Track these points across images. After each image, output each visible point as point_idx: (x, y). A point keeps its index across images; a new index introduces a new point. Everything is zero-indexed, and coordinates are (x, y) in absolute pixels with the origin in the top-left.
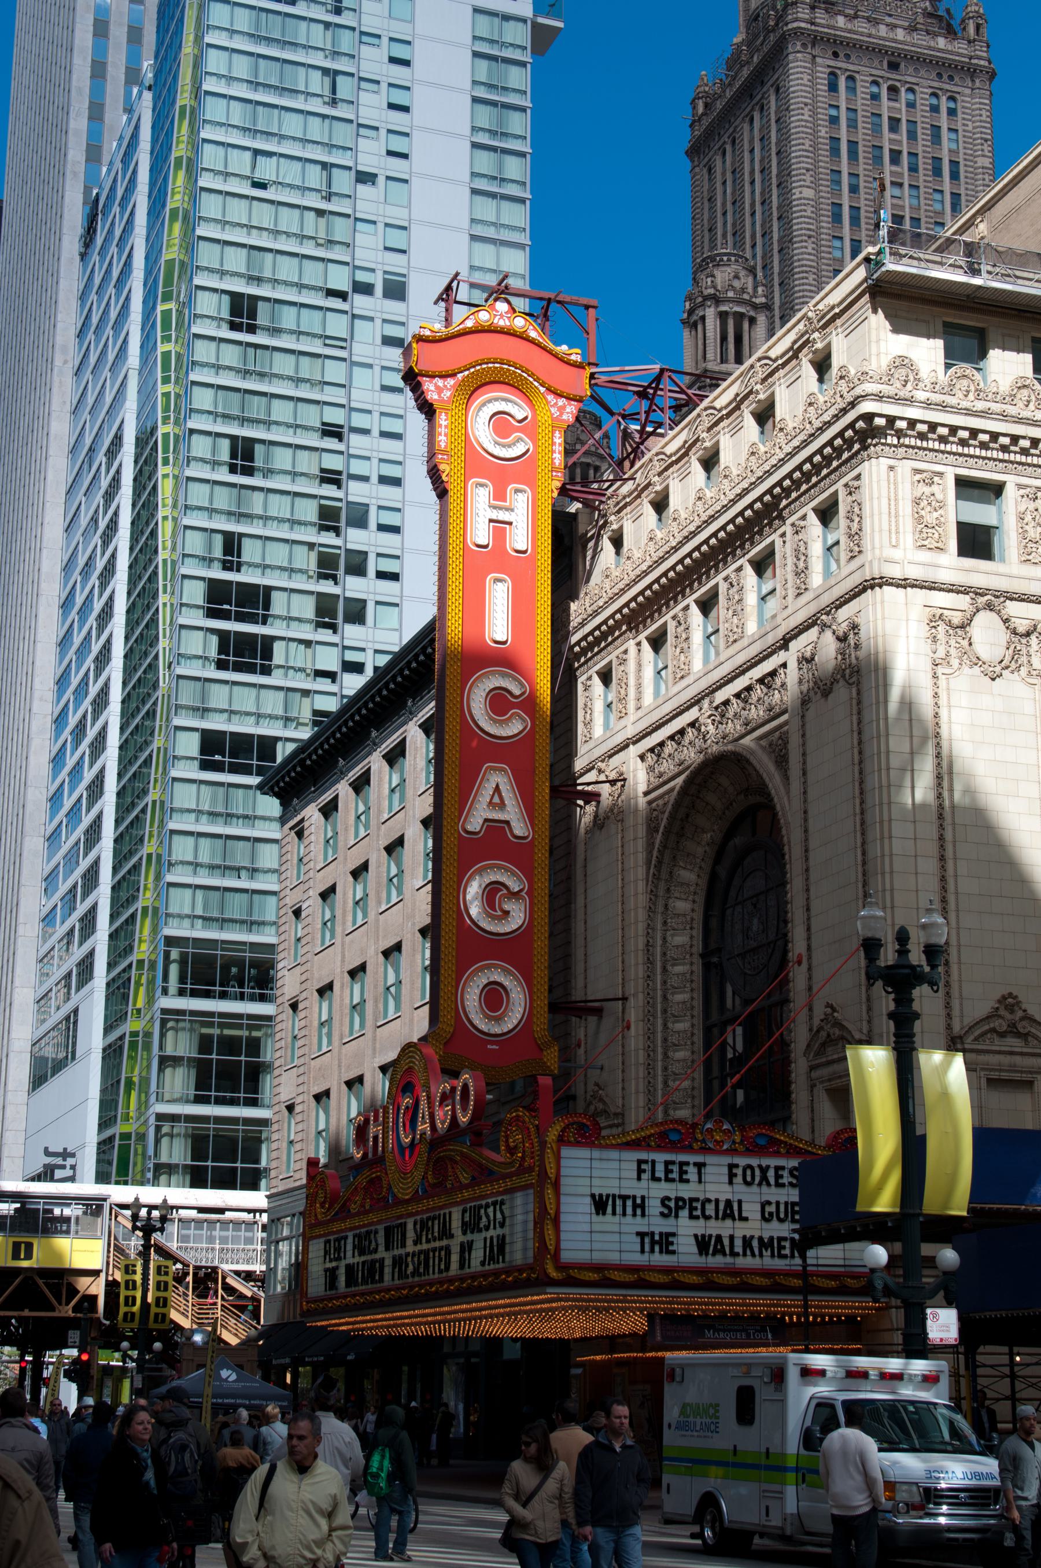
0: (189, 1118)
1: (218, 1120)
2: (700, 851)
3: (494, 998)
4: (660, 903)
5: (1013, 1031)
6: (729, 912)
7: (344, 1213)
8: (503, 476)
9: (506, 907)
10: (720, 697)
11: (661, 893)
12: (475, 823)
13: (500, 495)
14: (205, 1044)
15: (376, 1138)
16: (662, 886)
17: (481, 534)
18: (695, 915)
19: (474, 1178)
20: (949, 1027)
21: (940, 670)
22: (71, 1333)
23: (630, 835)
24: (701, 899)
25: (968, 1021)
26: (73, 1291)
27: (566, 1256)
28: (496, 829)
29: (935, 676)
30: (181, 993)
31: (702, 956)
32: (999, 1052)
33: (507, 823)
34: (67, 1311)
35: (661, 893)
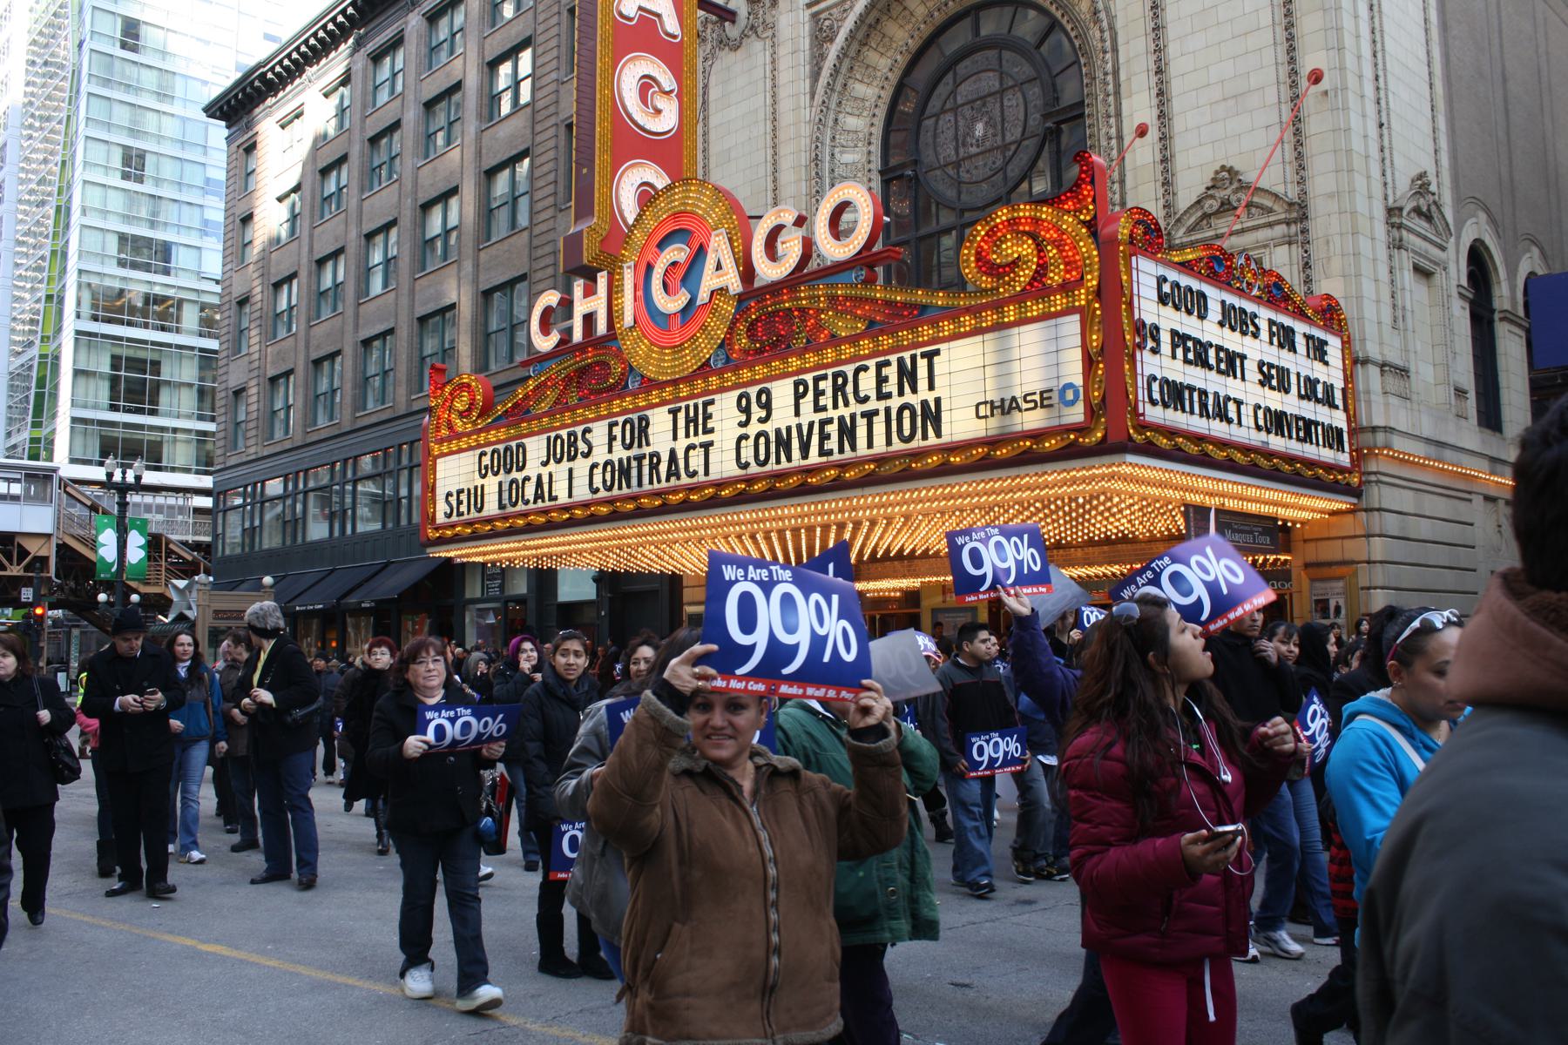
0: (101, 423)
1: (127, 425)
2: (883, 63)
4: (832, 116)
5: (1429, 218)
6: (929, 123)
7: (519, 415)
9: (659, 106)
11: (833, 106)
14: (116, 362)
15: (589, 319)
16: (835, 98)
18: (873, 130)
19: (872, 323)
22: (24, 590)
23: (783, 51)
24: (881, 113)
25: (1398, 194)
26: (24, 553)
28: (649, 19)
30: (95, 318)
31: (881, 173)
32: (1419, 235)
33: (659, 16)
34: (15, 570)
35: (833, 106)
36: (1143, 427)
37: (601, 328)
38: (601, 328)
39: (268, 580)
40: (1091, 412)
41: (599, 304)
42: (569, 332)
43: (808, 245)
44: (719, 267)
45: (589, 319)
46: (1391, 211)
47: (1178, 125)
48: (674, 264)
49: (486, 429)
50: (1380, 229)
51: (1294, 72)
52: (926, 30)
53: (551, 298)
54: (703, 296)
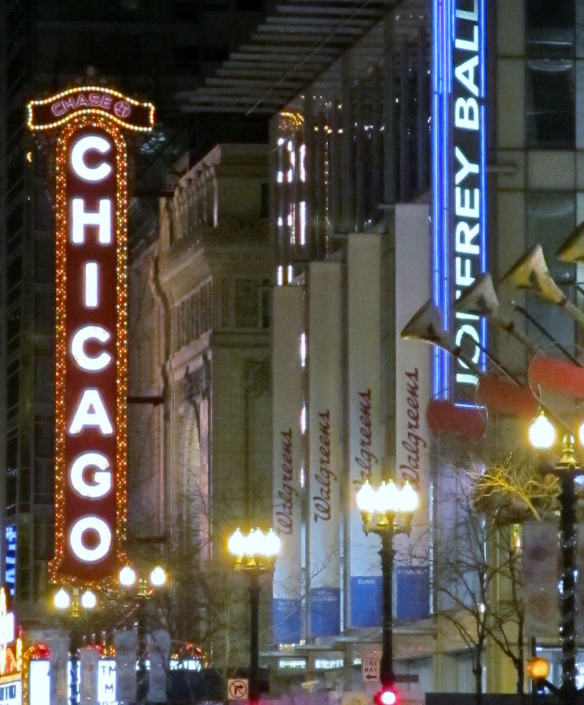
3: (91, 539)
8: (92, 194)
12: (75, 428)
13: (91, 207)
17: (78, 237)
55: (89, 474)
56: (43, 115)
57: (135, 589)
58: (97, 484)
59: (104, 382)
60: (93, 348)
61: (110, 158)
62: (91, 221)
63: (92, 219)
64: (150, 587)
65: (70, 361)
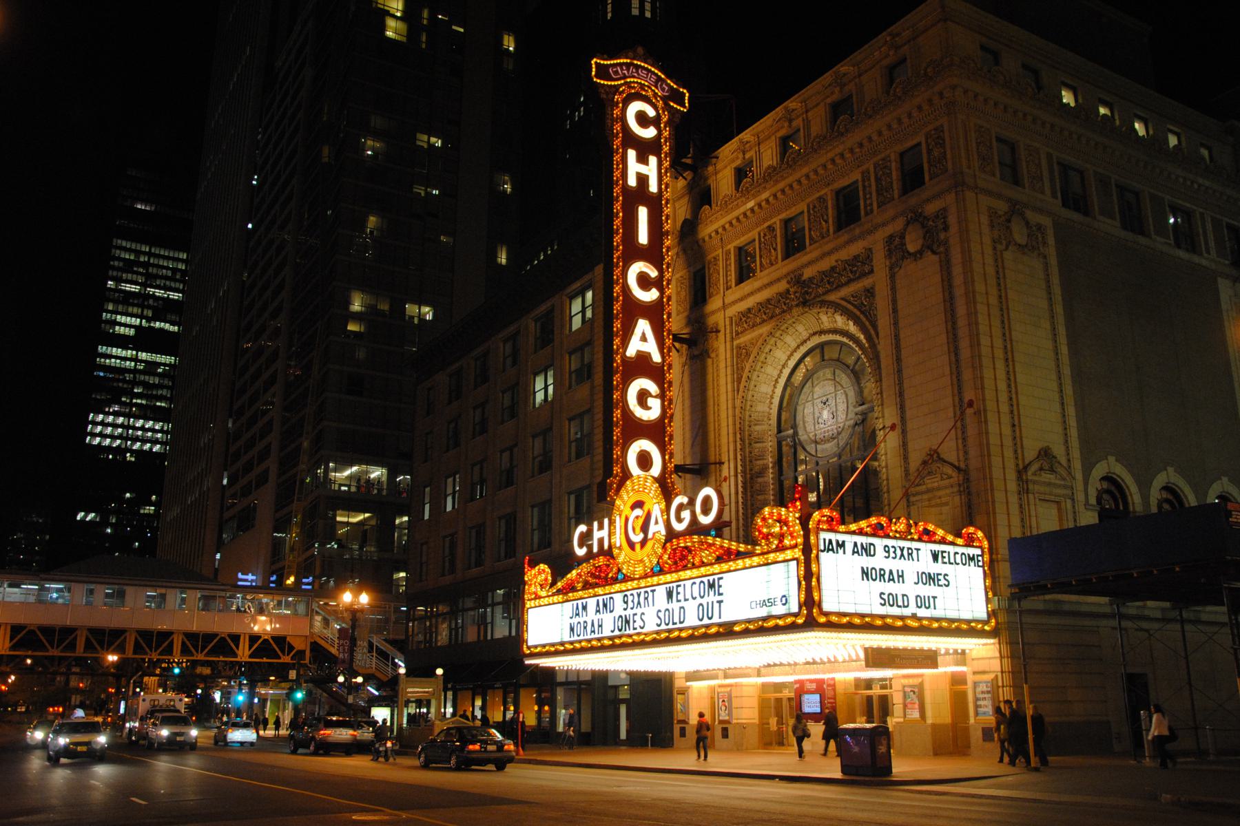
3: (644, 461)
8: (645, 149)
9: (649, 404)
10: (808, 273)
12: (631, 352)
13: (642, 159)
15: (601, 541)
17: (632, 181)
20: (1017, 465)
21: (999, 247)
26: (291, 648)
27: (826, 607)
28: (643, 357)
29: (995, 248)
34: (286, 659)
36: (827, 614)
37: (606, 546)
38: (606, 546)
39: (439, 671)
40: (800, 607)
41: (604, 533)
42: (590, 547)
43: (693, 514)
44: (657, 522)
45: (601, 541)
46: (1021, 472)
47: (909, 426)
48: (637, 517)
49: (553, 595)
50: (1012, 486)
51: (961, 400)
52: (797, 356)
53: (582, 528)
54: (650, 536)
55: (643, 396)
56: (603, 72)
57: (352, 604)
58: (649, 408)
59: (654, 312)
60: (644, 282)
61: (655, 122)
62: (640, 170)
63: (642, 169)
64: (359, 603)
65: (626, 289)
